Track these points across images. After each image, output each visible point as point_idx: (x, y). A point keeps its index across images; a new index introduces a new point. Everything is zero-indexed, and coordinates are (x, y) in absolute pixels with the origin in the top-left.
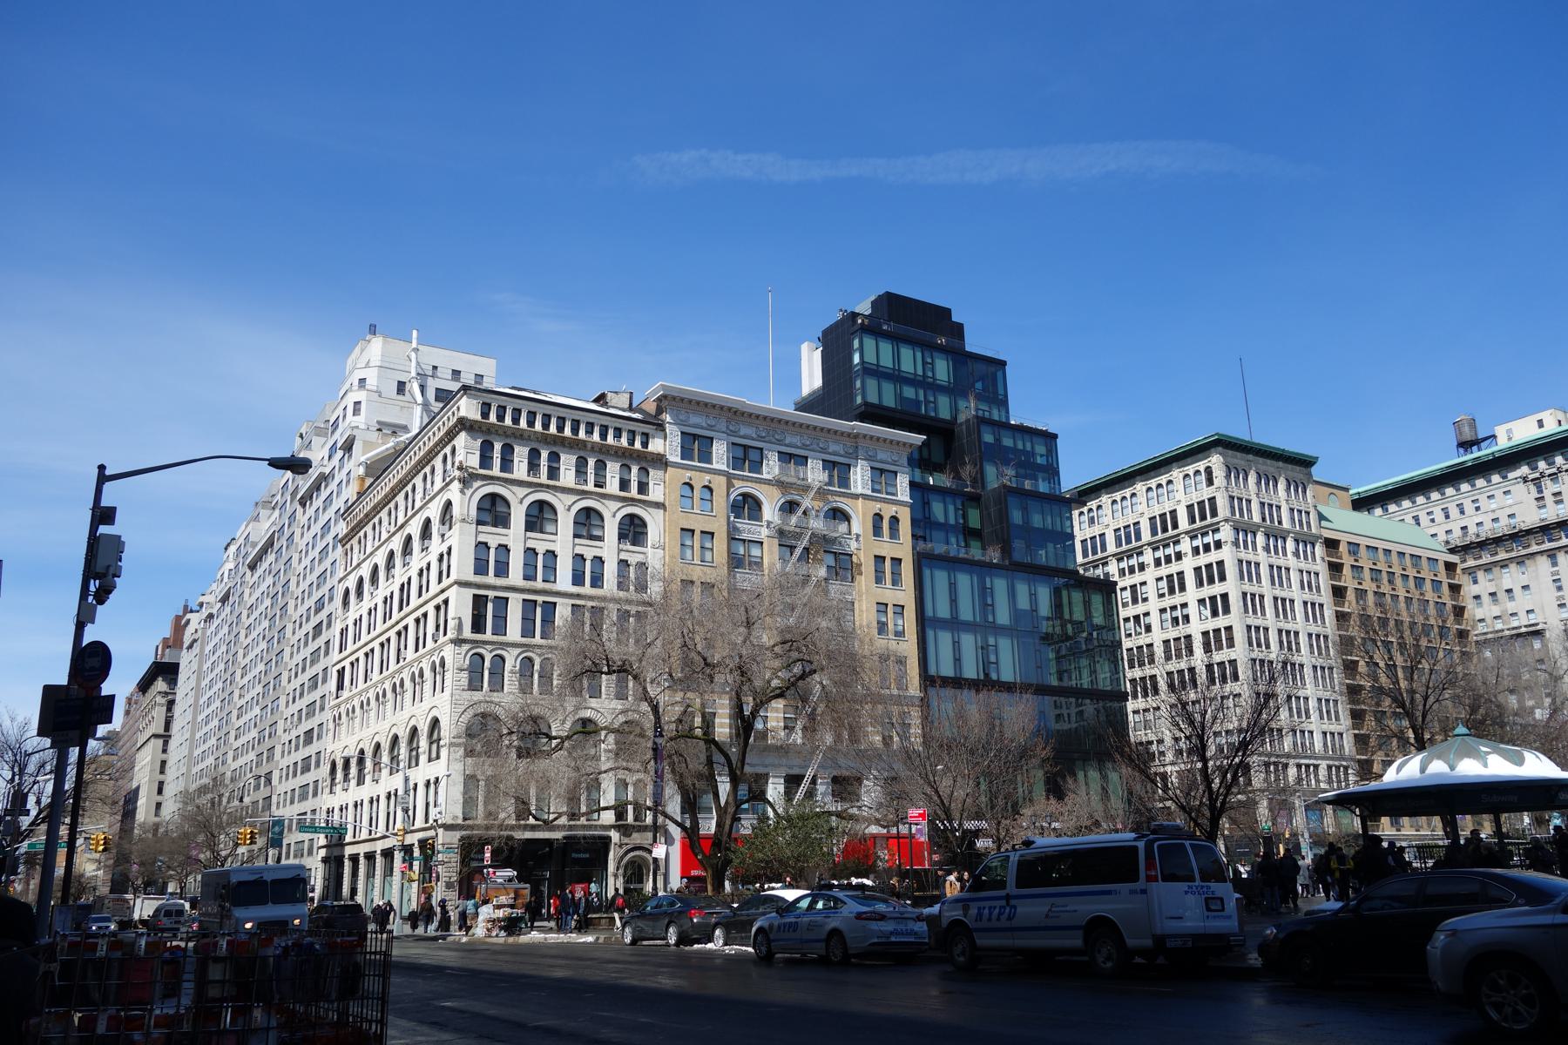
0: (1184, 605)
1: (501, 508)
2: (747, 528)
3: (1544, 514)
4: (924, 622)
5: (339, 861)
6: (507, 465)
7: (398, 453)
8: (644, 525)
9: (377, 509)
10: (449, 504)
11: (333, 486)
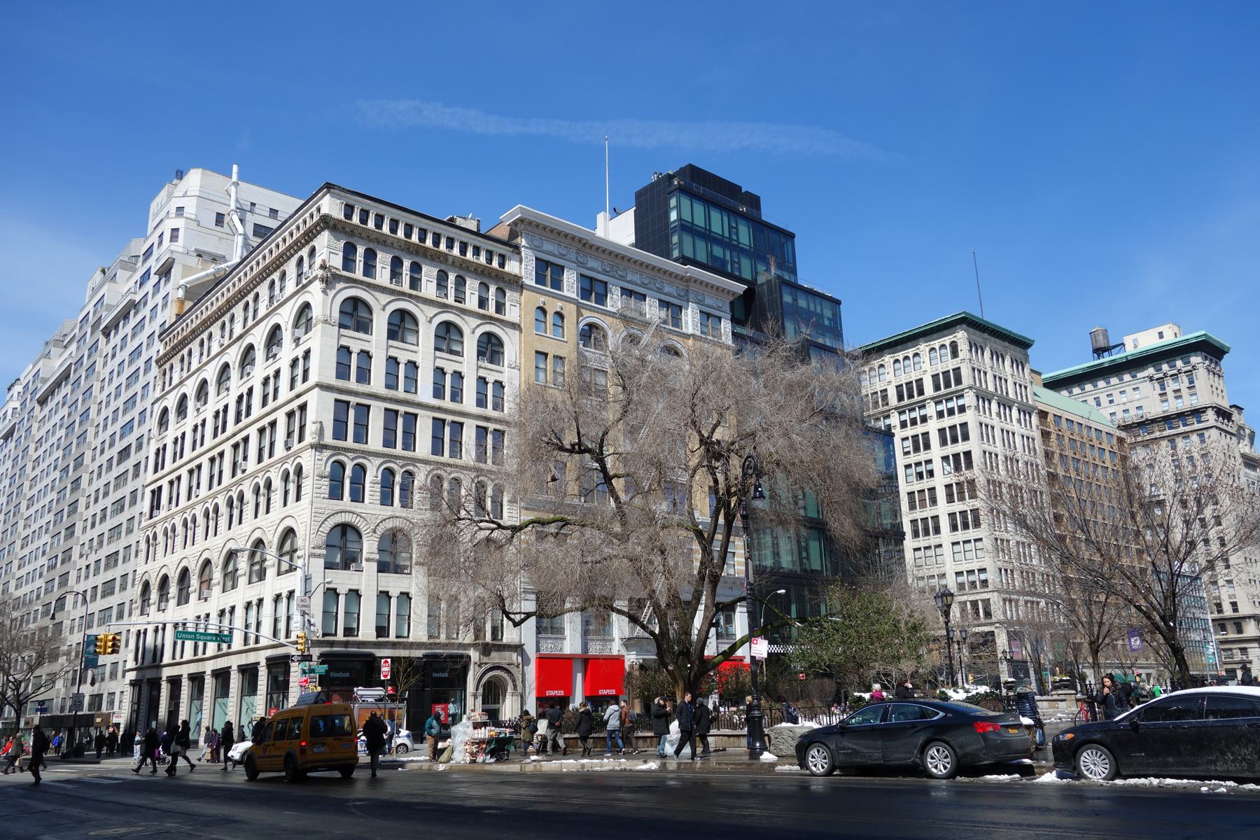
0: (929, 462)
1: (363, 313)
3: (1165, 406)
5: (155, 684)
6: (369, 269)
7: (218, 281)
8: (501, 344)
9: (207, 324)
10: (307, 306)
11: (145, 312)
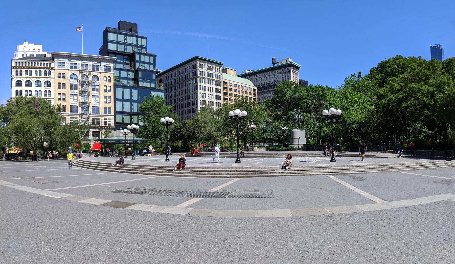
4: (116, 100)
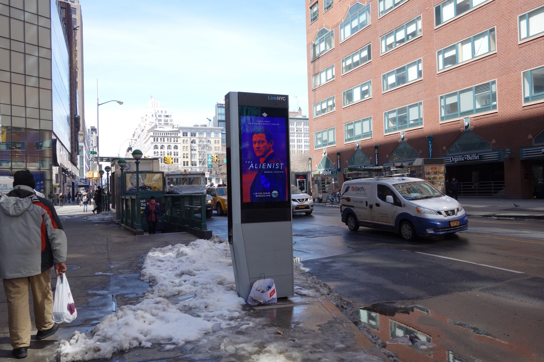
2: (193, 145)
6: (157, 141)
